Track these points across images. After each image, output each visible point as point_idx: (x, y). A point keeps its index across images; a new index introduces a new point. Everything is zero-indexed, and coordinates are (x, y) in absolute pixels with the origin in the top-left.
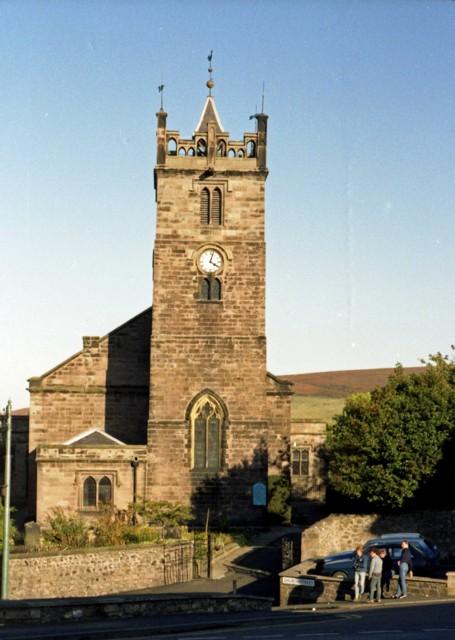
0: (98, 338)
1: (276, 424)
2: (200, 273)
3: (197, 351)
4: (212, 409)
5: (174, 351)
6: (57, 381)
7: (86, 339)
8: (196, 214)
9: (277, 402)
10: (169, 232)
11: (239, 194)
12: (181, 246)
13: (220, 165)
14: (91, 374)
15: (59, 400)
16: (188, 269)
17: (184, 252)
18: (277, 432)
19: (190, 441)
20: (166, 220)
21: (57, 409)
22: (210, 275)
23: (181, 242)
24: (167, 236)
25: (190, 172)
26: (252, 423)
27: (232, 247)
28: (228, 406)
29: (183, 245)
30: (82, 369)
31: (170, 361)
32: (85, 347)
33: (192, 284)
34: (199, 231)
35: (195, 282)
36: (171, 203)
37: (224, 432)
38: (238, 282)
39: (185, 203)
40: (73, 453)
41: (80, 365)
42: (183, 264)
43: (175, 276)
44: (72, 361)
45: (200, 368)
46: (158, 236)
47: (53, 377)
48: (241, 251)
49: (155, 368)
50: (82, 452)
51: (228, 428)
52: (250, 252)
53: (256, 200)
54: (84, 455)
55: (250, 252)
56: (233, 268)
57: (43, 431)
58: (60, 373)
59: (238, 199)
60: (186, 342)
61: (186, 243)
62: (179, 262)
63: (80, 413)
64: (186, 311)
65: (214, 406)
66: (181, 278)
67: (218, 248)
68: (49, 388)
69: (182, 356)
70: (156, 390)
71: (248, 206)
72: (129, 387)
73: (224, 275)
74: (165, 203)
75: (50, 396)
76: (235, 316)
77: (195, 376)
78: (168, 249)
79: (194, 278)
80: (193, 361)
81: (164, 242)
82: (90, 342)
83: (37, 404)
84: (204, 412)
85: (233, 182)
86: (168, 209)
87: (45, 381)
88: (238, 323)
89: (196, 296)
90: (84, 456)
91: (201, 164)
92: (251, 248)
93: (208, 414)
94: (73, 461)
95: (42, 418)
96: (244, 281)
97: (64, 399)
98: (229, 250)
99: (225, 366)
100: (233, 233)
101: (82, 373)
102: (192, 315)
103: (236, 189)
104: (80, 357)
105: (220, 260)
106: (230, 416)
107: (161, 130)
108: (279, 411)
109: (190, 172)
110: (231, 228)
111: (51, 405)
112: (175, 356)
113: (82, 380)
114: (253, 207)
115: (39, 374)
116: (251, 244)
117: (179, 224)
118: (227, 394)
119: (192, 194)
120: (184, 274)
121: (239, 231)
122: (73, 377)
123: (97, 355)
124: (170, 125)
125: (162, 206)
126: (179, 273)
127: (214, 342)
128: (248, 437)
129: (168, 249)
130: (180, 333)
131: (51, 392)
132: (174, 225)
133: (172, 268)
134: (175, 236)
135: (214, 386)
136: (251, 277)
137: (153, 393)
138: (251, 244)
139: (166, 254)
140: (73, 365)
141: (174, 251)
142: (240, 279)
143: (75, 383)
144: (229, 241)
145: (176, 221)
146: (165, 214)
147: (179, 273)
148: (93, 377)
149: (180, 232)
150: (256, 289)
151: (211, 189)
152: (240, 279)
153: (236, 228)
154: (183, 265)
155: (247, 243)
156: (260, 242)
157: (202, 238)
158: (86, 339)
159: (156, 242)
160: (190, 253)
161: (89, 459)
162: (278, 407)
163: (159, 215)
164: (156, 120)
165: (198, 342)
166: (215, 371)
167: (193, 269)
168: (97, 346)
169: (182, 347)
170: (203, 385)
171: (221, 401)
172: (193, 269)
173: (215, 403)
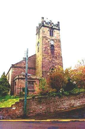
6: (17, 65)
12: (47, 39)
24: (44, 37)
25: (48, 27)
42: (47, 42)
45: (52, 61)
57: (14, 75)
62: (47, 41)
67: (53, 40)
69: (48, 58)
75: (16, 68)
78: (45, 39)
80: (50, 60)
85: (55, 30)
86: (44, 32)
89: (50, 48)
99: (56, 61)
100: (55, 38)
109: (48, 27)
112: (47, 58)
119: (48, 30)
129: (45, 39)
131: (16, 67)
134: (46, 37)
144: (55, 39)
145: (46, 34)
146: (44, 33)
149: (47, 36)
151: (51, 31)
166: (54, 62)
167: (49, 43)
172: (49, 43)
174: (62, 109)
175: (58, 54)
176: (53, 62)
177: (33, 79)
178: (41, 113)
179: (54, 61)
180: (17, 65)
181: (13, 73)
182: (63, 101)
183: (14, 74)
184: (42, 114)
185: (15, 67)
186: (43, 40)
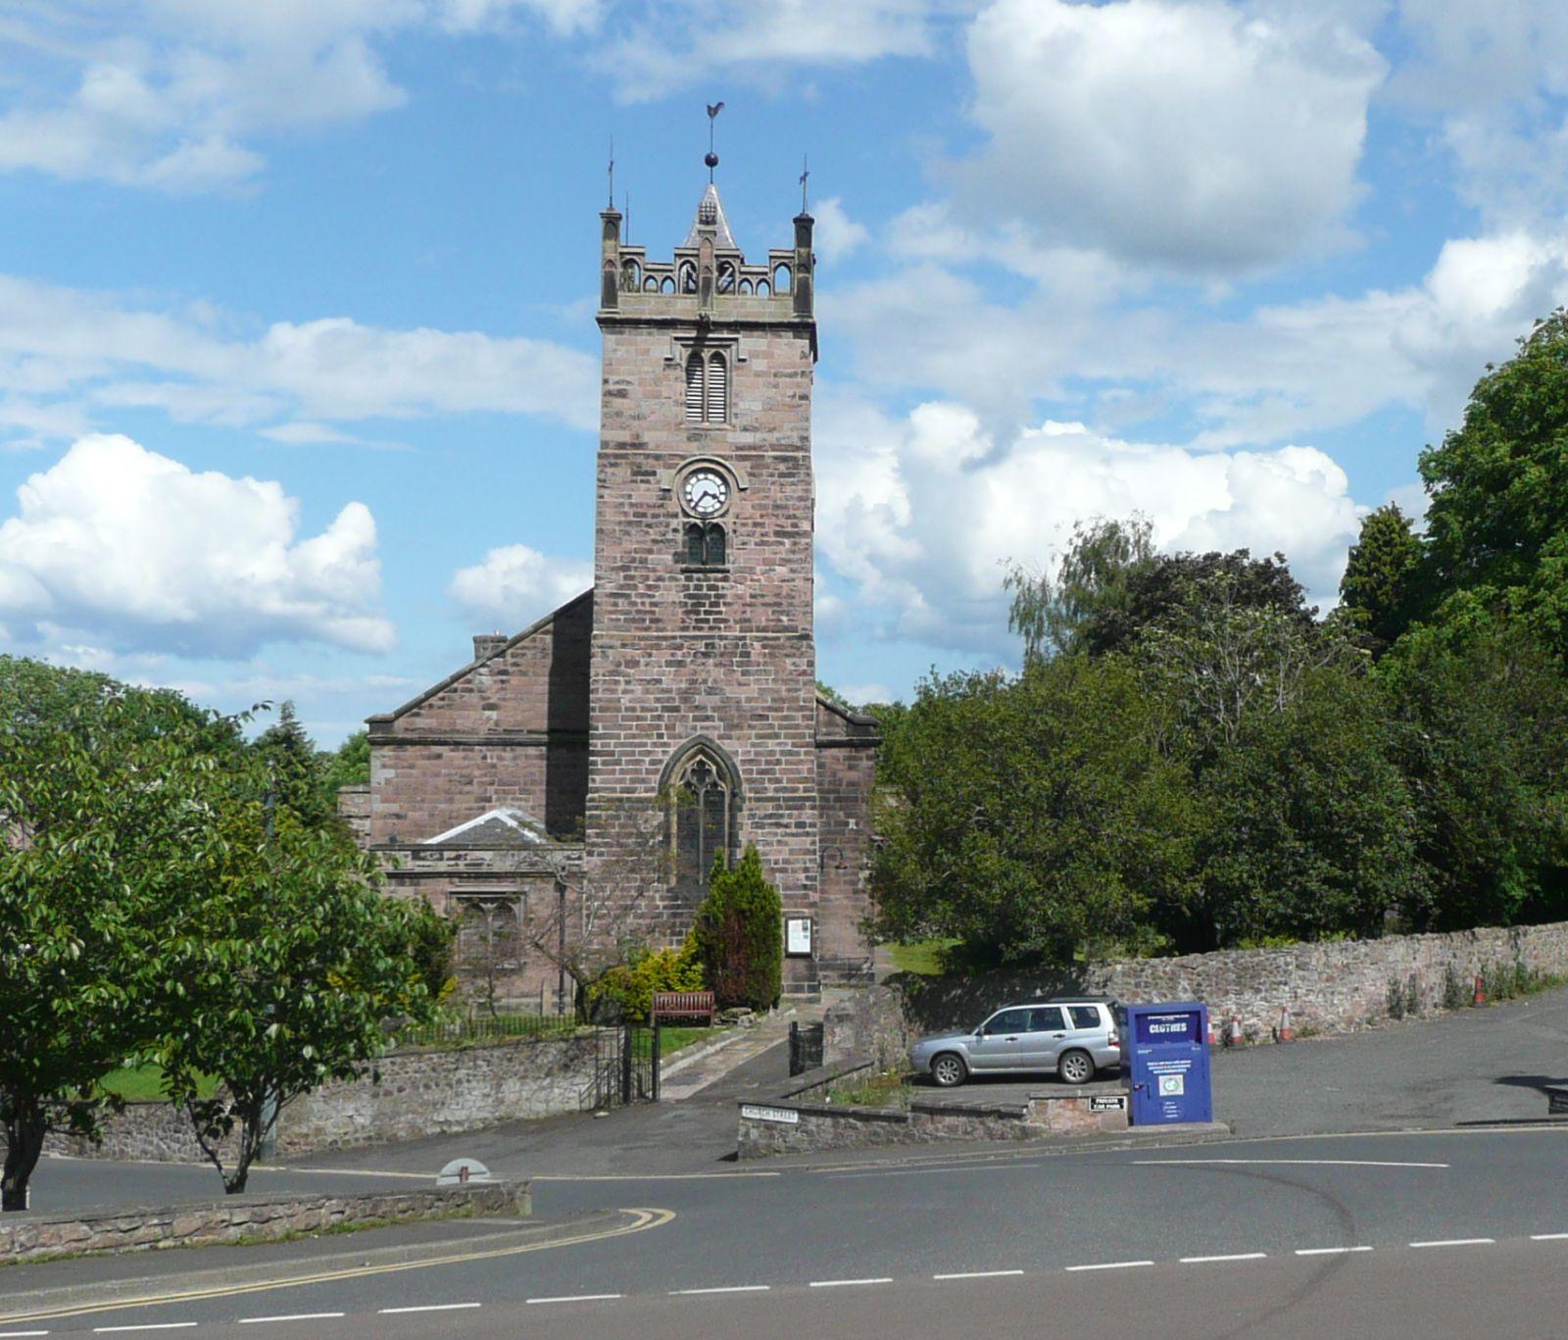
0: (503, 640)
1: (847, 799)
2: (687, 515)
3: (680, 664)
4: (710, 771)
5: (635, 664)
6: (420, 723)
7: (479, 642)
8: (677, 403)
9: (849, 758)
10: (625, 436)
11: (759, 365)
13: (722, 309)
14: (491, 707)
15: (429, 758)
16: (662, 506)
17: (654, 474)
18: (849, 816)
19: (667, 837)
20: (619, 414)
21: (424, 774)
22: (704, 516)
23: (647, 456)
24: (622, 445)
26: (786, 799)
27: (748, 464)
28: (740, 768)
29: (651, 461)
30: (474, 698)
31: (628, 682)
32: (477, 657)
33: (670, 536)
34: (685, 435)
35: (675, 530)
36: (628, 383)
37: (733, 817)
38: (759, 530)
39: (656, 382)
40: (441, 859)
41: (471, 690)
43: (640, 518)
44: (455, 685)
45: (686, 696)
46: (605, 444)
47: (417, 715)
48: (764, 471)
49: (598, 696)
50: (458, 858)
51: (741, 810)
52: (782, 475)
53: (790, 376)
54: (461, 863)
55: (782, 475)
56: (748, 504)
57: (398, 816)
58: (431, 706)
59: (758, 374)
60: (658, 647)
61: (657, 457)
62: (645, 494)
63: (470, 783)
64: (657, 587)
65: (714, 768)
66: (649, 526)
68: (408, 736)
70: (600, 737)
71: (776, 386)
72: (566, 731)
73: (730, 518)
74: (618, 383)
75: (411, 751)
76: (752, 596)
77: (676, 709)
78: (623, 472)
79: (674, 523)
81: (617, 456)
82: (495, 649)
83: (384, 766)
84: (694, 781)
85: (747, 343)
86: (622, 394)
87: (400, 723)
88: (760, 609)
89: (678, 558)
90: (462, 867)
91: (686, 307)
92: (782, 467)
93: (701, 780)
94: (440, 875)
95: (397, 792)
96: (771, 530)
97: (439, 756)
98: (740, 470)
99: (730, 691)
100: (748, 438)
101: (473, 707)
102: (671, 594)
103: (755, 355)
104: (469, 676)
105: (719, 481)
106: (745, 786)
107: (612, 243)
108: (853, 775)
110: (745, 429)
111: (412, 767)
113: (475, 720)
114: (788, 388)
115: (387, 710)
116: (784, 459)
117: (644, 424)
118: (738, 749)
120: (654, 516)
121: (759, 436)
122: (455, 714)
123: (504, 672)
124: (632, 236)
125: (611, 387)
126: (644, 515)
127: (713, 646)
128: (778, 825)
129: (623, 472)
130: (647, 629)
132: (636, 423)
133: (632, 505)
135: (714, 731)
136: (782, 521)
137: (597, 744)
138: (784, 459)
139: (619, 480)
140: (455, 690)
141: (635, 474)
142: (762, 525)
143: (460, 724)
144: (744, 454)
145: (638, 417)
146: (618, 402)
147: (644, 515)
148: (494, 714)
149: (645, 438)
150: (795, 544)
152: (762, 525)
153: (755, 429)
154: (654, 501)
155: (775, 458)
156: (800, 454)
157: (694, 450)
158: (479, 642)
159: (600, 456)
160: (666, 477)
161: (471, 870)
162: (851, 768)
163: (605, 405)
164: (600, 224)
165: (680, 647)
166: (715, 700)
167: (672, 506)
168: (501, 654)
169: (650, 655)
170: (694, 728)
171: (727, 757)
173: (716, 763)
174: (455, 1129)
175: (762, 617)
176: (698, 699)
177: (499, 876)
178: (348, 1141)
179: (710, 692)
180: (420, 722)
181: (383, 802)
182: (459, 1081)
183: (394, 808)
184: (353, 1144)
185: (401, 743)
186: (602, 484)
